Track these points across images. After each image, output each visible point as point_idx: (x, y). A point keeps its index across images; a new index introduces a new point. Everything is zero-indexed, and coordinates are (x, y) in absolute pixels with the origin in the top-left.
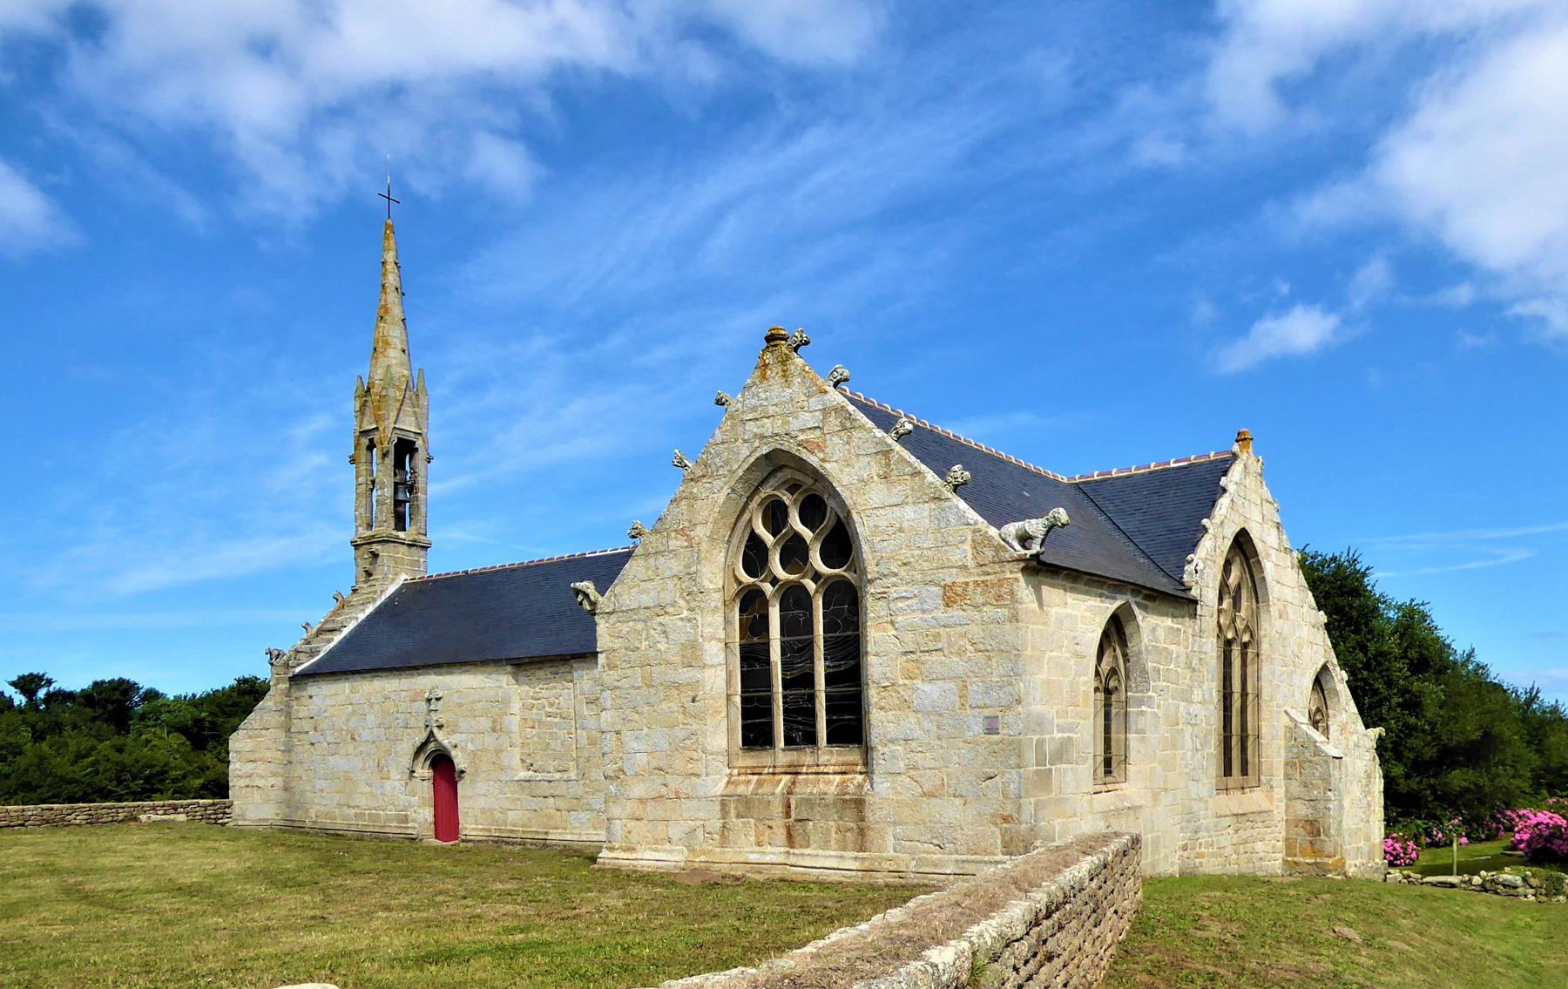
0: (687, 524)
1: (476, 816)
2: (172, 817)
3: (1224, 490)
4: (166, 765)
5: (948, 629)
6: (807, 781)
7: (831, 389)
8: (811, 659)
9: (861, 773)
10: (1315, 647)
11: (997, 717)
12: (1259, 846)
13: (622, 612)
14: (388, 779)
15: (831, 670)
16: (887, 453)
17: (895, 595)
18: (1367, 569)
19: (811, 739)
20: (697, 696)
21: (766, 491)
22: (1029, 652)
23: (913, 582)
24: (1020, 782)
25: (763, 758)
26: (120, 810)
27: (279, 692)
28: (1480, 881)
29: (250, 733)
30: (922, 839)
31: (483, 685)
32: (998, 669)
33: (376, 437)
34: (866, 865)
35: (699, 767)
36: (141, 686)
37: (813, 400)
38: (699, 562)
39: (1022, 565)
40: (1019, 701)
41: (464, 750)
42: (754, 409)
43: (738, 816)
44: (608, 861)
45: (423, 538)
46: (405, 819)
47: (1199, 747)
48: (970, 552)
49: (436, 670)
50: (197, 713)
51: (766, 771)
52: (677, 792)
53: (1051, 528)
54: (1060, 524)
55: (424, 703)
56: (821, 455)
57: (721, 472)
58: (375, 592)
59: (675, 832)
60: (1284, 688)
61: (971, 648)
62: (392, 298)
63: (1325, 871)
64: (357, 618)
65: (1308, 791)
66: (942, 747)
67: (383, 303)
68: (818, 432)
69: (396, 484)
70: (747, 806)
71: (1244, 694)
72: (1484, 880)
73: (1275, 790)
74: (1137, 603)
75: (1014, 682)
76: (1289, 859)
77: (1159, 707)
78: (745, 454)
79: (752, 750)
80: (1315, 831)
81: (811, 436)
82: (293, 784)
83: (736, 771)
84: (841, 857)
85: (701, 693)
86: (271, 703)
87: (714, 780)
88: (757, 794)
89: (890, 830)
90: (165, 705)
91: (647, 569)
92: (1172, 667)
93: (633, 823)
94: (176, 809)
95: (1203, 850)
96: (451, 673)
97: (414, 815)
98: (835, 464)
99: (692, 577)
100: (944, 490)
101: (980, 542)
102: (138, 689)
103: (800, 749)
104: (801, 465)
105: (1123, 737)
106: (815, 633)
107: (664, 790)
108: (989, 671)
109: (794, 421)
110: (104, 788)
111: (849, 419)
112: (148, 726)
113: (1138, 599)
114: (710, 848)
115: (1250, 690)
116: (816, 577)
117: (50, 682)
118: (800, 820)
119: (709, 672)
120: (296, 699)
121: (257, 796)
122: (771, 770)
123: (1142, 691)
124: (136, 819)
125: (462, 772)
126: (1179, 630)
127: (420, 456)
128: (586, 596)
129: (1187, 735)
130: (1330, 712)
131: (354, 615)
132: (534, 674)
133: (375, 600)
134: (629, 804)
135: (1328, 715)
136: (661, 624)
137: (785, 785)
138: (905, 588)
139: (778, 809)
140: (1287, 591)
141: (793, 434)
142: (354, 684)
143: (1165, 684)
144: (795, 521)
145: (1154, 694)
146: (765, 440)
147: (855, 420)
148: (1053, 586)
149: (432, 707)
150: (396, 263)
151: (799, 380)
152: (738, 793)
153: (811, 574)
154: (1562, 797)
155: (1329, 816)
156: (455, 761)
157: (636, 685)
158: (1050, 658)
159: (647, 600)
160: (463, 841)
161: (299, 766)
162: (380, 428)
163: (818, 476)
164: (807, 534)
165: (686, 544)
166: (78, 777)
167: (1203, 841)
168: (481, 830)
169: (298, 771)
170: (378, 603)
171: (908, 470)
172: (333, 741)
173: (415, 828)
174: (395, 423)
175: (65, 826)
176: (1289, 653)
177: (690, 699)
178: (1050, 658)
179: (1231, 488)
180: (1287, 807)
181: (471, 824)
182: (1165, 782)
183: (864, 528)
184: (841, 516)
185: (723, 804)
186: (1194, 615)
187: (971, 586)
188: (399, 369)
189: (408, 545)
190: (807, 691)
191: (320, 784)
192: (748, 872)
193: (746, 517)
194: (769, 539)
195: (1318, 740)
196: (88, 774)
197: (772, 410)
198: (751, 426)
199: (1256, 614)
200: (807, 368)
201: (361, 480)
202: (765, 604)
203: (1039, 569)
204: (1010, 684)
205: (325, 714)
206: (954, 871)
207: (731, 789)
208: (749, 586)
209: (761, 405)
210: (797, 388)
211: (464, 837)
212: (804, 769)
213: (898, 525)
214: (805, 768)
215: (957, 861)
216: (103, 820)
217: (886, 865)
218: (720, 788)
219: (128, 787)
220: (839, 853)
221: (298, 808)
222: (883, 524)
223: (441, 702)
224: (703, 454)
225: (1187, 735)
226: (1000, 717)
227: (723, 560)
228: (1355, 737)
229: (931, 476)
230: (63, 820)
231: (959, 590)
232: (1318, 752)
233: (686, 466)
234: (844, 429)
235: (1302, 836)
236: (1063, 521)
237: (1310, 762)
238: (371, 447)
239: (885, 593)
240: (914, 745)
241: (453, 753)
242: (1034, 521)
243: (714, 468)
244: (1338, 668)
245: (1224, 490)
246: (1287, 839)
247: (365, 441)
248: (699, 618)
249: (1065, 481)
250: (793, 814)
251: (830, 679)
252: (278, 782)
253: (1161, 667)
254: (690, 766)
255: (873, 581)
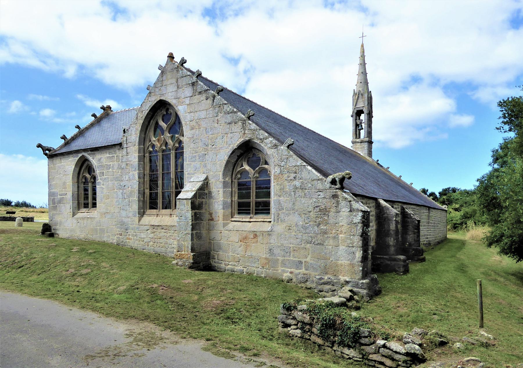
74: (89, 154)
95: (130, 237)
113: (89, 153)
167: (130, 233)
253: (104, 171)
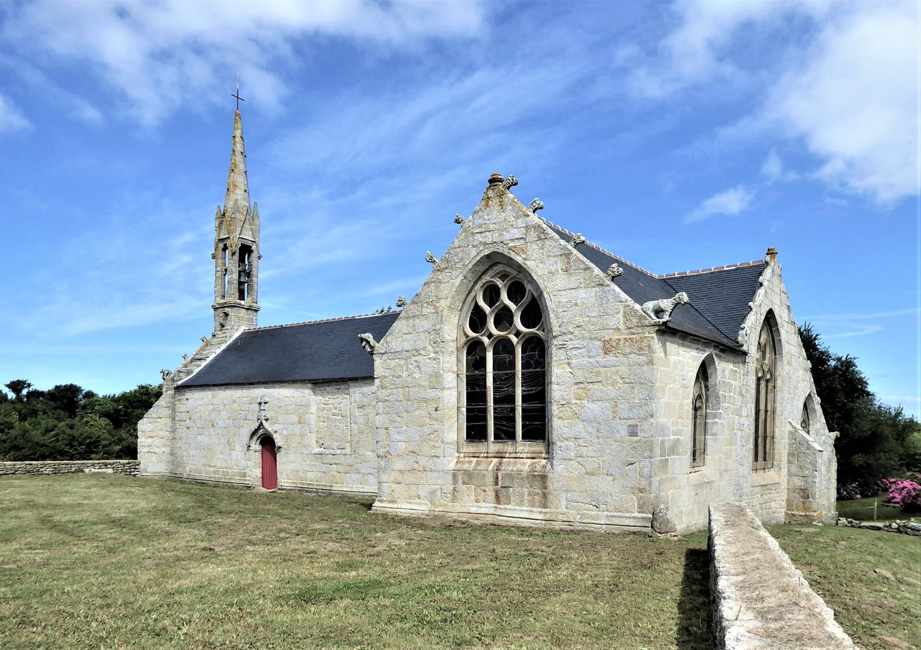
0: (434, 298)
1: (288, 475)
2: (104, 470)
3: (761, 285)
4: (99, 437)
5: (606, 369)
6: (509, 463)
7: (531, 214)
8: (513, 386)
9: (545, 459)
10: (805, 383)
11: (637, 425)
12: (773, 504)
13: (391, 353)
14: (234, 450)
15: (526, 393)
16: (568, 255)
17: (571, 346)
18: (817, 335)
19: (512, 436)
20: (438, 407)
21: (486, 278)
22: (658, 384)
23: (584, 338)
24: (651, 467)
25: (480, 447)
26: (73, 466)
27: (168, 396)
28: (897, 526)
29: (150, 420)
30: (585, 501)
31: (293, 395)
32: (638, 396)
33: (228, 243)
34: (547, 517)
35: (439, 452)
36: (83, 389)
37: (519, 220)
38: (442, 322)
39: (657, 328)
40: (652, 416)
41: (281, 434)
42: (480, 226)
43: (464, 483)
44: (379, 508)
45: (255, 304)
46: (244, 475)
47: (744, 444)
48: (622, 319)
49: (264, 385)
50: (116, 406)
51: (482, 455)
52: (424, 467)
53: (676, 305)
54: (683, 303)
55: (257, 405)
56: (524, 256)
57: (457, 266)
58: (226, 337)
59: (423, 492)
60: (789, 407)
61: (621, 381)
62: (239, 158)
63: (812, 520)
64: (215, 353)
65: (802, 471)
66: (599, 444)
67: (233, 161)
68: (522, 241)
69: (240, 272)
70: (470, 477)
71: (766, 411)
72: (899, 526)
73: (783, 470)
74: (716, 355)
75: (649, 403)
76: (789, 512)
77: (724, 420)
78: (474, 255)
79: (473, 442)
80: (806, 495)
81: (517, 243)
82: (176, 451)
83: (462, 455)
84: (531, 511)
85: (441, 405)
86: (163, 403)
87: (448, 461)
88: (477, 470)
89: (564, 495)
90: (97, 401)
91: (408, 326)
92: (732, 394)
93: (396, 485)
94: (106, 466)
96: (274, 387)
97: (250, 473)
98: (533, 262)
99: (437, 332)
100: (605, 279)
101: (629, 314)
102: (82, 390)
103: (505, 442)
104: (510, 261)
105: (703, 438)
106: (517, 369)
107: (416, 466)
108: (633, 396)
109: (507, 234)
110: (63, 450)
111: (543, 233)
112: (87, 413)
114: (445, 502)
115: (769, 409)
116: (518, 334)
117: (29, 385)
118: (505, 487)
119: (446, 392)
120: (178, 400)
121: (154, 457)
122: (485, 455)
123: (716, 410)
124: (82, 471)
125: (280, 447)
126: (736, 371)
127: (254, 255)
128: (368, 342)
129: (738, 437)
130: (811, 422)
131: (213, 350)
132: (325, 389)
133: (226, 342)
134: (393, 473)
135: (809, 425)
136: (416, 361)
137: (495, 465)
138: (578, 342)
139: (490, 479)
140: (793, 348)
141: (506, 242)
142: (214, 392)
143: (728, 405)
144: (504, 297)
145: (722, 411)
146: (487, 246)
147: (548, 234)
148: (672, 342)
149: (262, 408)
150: (241, 137)
151: (511, 208)
152: (464, 468)
153: (514, 332)
154: (914, 472)
155: (815, 487)
156: (276, 441)
157: (399, 399)
158: (670, 388)
159: (407, 346)
160: (279, 489)
161: (180, 441)
162: (231, 238)
163: (521, 269)
164: (512, 306)
165: (434, 311)
166: (46, 443)
168: (291, 483)
169: (179, 444)
170: (228, 344)
171: (582, 266)
172: (201, 426)
173: (250, 480)
174: (240, 235)
175: (40, 474)
176: (792, 386)
177: (434, 409)
178: (670, 388)
179: (765, 283)
180: (789, 481)
181: (285, 480)
182: (727, 466)
183: (552, 303)
184: (535, 294)
185: (454, 476)
186: (744, 362)
187: (622, 341)
188: (243, 202)
189: (246, 309)
190: (510, 406)
191: (193, 452)
192: (470, 518)
193: (473, 294)
194: (487, 309)
195: (810, 440)
196: (53, 441)
197: (492, 227)
198: (478, 237)
199: (774, 363)
200: (516, 200)
201: (218, 269)
202: (484, 350)
203: (666, 331)
204: (647, 405)
205: (196, 410)
206: (606, 523)
207: (459, 466)
208: (473, 338)
209: (485, 224)
210: (509, 213)
211: (280, 487)
212: (507, 455)
213: (574, 302)
214: (508, 454)
215: (607, 516)
216: (63, 471)
217: (560, 517)
218: (452, 465)
219: (76, 450)
220: (530, 509)
221: (178, 466)
222: (564, 300)
223: (267, 405)
224: (446, 254)
225: (738, 437)
226: (639, 426)
227: (457, 321)
228: (824, 438)
229: (597, 271)
230: (38, 471)
231: (614, 344)
232: (809, 447)
233: (435, 261)
234: (540, 239)
235: (798, 499)
236: (685, 301)
237: (804, 453)
238: (225, 248)
239: (565, 345)
240: (581, 442)
241: (275, 436)
242: (665, 300)
243: (453, 263)
244: (816, 396)
245: (761, 285)
246: (788, 500)
247: (221, 245)
248: (441, 358)
249: (657, 277)
250: (500, 483)
251: (525, 399)
252: (167, 450)
253: (727, 394)
254: (433, 451)
255: (557, 337)
